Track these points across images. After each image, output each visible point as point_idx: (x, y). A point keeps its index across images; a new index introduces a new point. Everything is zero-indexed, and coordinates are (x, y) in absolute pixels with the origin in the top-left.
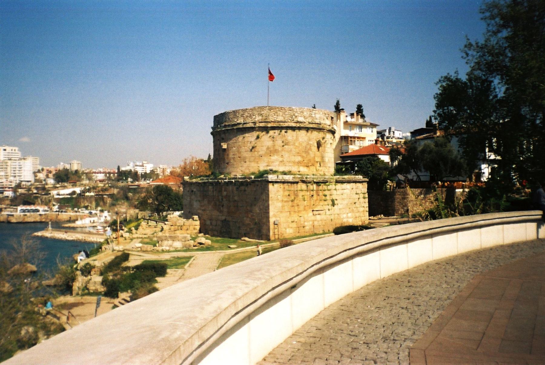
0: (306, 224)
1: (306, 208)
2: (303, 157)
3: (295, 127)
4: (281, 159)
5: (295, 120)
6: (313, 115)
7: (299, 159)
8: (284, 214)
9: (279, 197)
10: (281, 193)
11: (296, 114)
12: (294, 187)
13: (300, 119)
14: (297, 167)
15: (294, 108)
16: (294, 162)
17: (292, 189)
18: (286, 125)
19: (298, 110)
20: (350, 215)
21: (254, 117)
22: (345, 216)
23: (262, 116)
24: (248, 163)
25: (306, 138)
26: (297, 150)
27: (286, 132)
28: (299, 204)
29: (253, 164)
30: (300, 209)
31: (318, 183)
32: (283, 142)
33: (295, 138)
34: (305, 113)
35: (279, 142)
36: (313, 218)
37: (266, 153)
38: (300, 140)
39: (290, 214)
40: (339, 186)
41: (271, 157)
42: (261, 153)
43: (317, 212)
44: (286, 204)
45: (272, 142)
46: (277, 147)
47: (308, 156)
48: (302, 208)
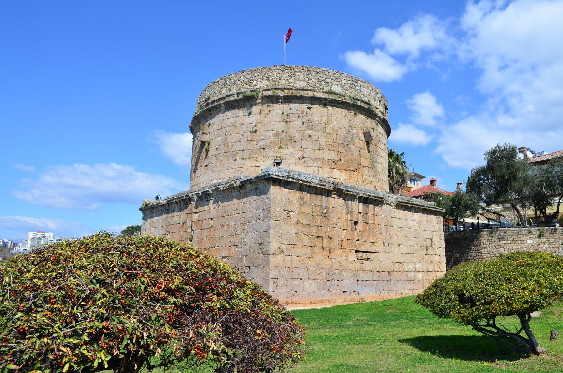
0: (344, 275)
1: (345, 243)
2: (339, 153)
3: (326, 99)
4: (299, 154)
5: (326, 89)
6: (358, 88)
7: (333, 156)
8: (299, 251)
9: (290, 213)
10: (296, 206)
11: (329, 80)
12: (321, 200)
13: (335, 88)
14: (328, 170)
15: (324, 69)
16: (323, 160)
17: (319, 203)
18: (310, 94)
19: (331, 74)
20: (418, 266)
21: (255, 82)
22: (411, 267)
23: (269, 81)
24: (239, 161)
25: (345, 123)
26: (329, 141)
27: (309, 108)
28: (331, 234)
29: (249, 163)
30: (332, 245)
31: (365, 200)
32: (303, 123)
33: (325, 119)
34: (344, 81)
35: (296, 124)
36: (357, 265)
37: (272, 143)
38: (335, 124)
39: (313, 252)
40: (401, 213)
41: (282, 150)
42: (262, 143)
43: (364, 256)
44: (305, 230)
45: (284, 124)
46: (293, 133)
47: (349, 153)
48: (336, 243)
